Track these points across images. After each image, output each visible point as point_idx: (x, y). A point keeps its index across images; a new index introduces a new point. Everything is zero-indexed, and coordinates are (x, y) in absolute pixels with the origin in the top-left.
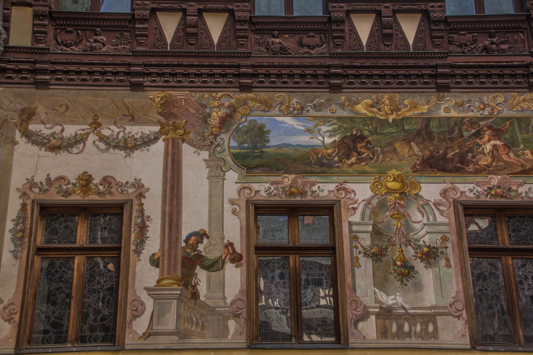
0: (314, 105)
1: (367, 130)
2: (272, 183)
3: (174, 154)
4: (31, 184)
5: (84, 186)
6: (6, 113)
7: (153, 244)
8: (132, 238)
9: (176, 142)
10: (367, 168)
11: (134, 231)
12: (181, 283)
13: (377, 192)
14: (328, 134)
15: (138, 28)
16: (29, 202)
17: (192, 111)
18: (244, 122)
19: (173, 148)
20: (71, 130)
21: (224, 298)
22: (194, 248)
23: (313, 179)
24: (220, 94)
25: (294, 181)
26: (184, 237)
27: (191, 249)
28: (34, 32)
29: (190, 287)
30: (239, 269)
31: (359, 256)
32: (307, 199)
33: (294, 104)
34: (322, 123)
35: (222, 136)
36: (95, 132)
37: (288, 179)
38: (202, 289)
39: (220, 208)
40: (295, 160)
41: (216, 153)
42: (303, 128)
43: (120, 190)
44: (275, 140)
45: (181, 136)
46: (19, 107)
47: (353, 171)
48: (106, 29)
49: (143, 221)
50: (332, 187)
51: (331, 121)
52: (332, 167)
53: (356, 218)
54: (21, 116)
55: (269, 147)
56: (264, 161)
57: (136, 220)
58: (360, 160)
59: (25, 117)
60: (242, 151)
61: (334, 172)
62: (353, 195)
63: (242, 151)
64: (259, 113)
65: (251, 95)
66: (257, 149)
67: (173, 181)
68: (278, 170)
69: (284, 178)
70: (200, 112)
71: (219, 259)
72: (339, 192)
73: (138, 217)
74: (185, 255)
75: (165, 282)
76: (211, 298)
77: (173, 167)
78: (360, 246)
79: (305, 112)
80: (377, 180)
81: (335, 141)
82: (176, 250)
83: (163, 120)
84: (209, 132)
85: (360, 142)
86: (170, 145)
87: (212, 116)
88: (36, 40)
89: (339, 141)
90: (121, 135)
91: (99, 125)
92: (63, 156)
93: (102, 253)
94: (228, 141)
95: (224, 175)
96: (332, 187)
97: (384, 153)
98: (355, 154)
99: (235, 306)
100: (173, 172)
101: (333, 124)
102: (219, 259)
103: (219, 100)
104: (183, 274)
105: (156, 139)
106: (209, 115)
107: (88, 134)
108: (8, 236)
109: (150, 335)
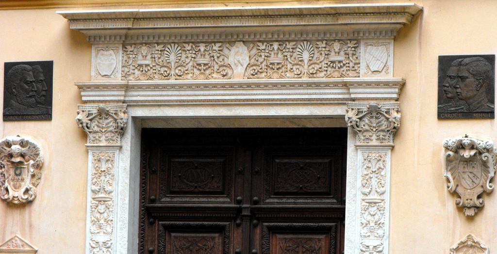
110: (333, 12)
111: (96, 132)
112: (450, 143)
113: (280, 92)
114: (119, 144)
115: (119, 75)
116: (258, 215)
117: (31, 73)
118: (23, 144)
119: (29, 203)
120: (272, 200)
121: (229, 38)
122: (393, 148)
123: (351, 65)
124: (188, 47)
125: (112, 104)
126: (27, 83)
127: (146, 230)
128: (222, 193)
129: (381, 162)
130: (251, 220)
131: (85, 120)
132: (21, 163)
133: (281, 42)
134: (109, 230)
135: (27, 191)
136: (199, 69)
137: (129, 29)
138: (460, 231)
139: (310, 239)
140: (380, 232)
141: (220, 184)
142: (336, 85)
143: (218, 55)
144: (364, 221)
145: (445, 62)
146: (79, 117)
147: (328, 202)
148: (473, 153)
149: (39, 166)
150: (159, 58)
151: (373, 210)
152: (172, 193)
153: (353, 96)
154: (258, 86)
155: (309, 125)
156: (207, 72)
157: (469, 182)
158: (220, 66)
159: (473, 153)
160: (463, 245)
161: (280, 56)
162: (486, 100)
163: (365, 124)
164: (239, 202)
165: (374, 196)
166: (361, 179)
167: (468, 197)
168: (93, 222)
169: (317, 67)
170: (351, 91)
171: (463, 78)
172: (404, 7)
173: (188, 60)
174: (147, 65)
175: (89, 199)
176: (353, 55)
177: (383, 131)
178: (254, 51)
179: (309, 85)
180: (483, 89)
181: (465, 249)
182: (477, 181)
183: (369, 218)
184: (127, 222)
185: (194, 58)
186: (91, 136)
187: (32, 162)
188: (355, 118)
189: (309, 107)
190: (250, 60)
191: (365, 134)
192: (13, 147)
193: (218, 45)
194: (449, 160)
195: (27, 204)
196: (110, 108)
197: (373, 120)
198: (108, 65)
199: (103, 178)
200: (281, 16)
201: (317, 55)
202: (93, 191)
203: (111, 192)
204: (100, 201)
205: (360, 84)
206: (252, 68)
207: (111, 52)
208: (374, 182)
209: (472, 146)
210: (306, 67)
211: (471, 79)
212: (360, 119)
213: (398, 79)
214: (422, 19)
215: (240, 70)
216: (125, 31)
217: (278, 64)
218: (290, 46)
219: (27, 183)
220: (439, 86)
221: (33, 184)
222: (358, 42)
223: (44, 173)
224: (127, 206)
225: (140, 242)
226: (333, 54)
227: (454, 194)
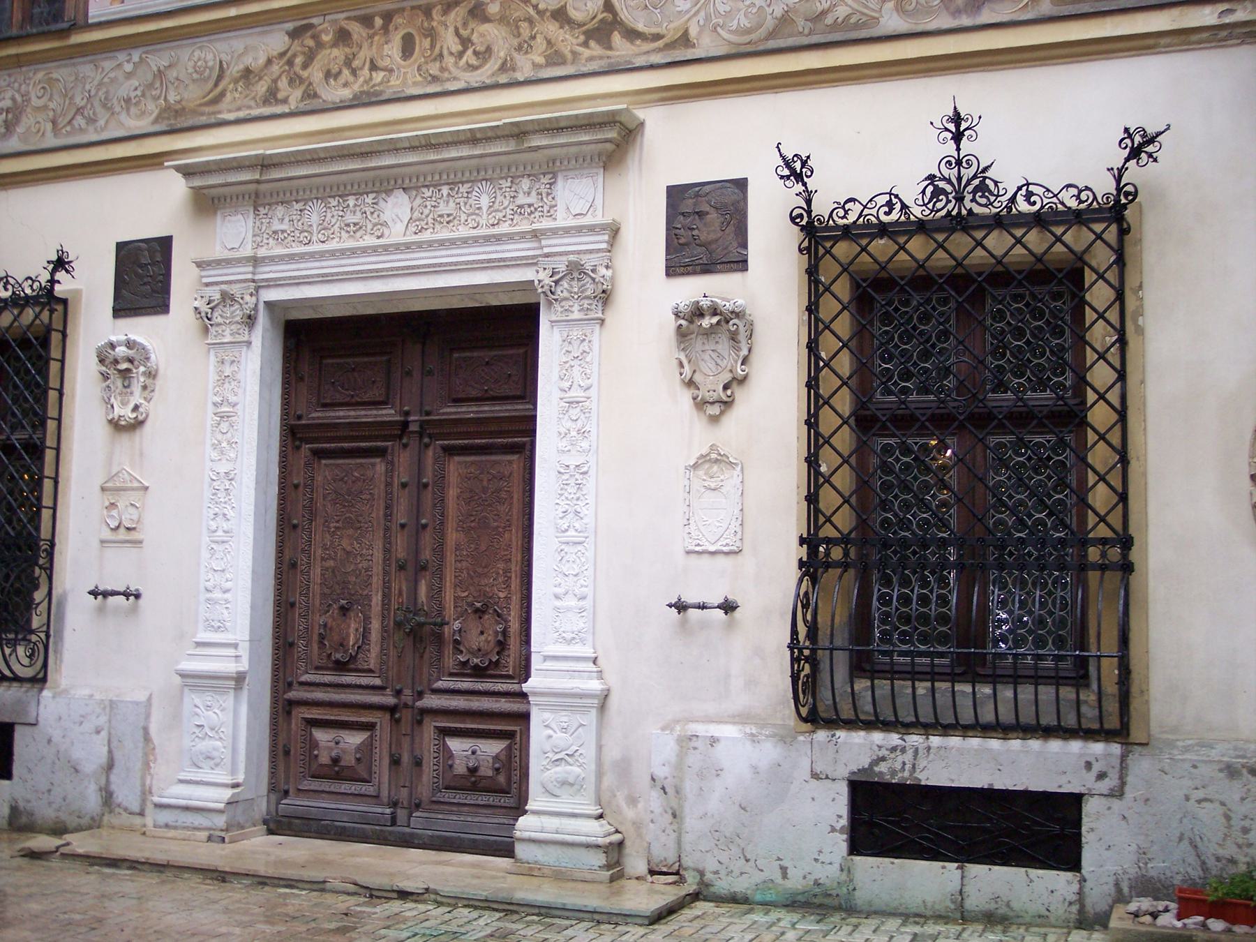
110: (516, 130)
111: (219, 325)
112: (681, 308)
113: (449, 252)
114: (246, 339)
115: (249, 247)
116: (430, 431)
117: (146, 253)
118: (130, 344)
119: (142, 423)
120: (448, 410)
121: (384, 185)
122: (602, 322)
123: (546, 208)
124: (334, 202)
125: (238, 286)
126: (141, 266)
127: (290, 458)
128: (386, 403)
129: (585, 343)
130: (421, 437)
131: (205, 308)
132: (128, 370)
133: (452, 184)
134: (233, 455)
135: (136, 408)
137: (258, 182)
138: (699, 436)
139: (496, 462)
140: (585, 444)
141: (383, 391)
142: (522, 236)
144: (563, 430)
145: (676, 194)
146: (197, 304)
147: (519, 408)
148: (715, 320)
149: (152, 375)
151: (574, 413)
152: (325, 405)
153: (546, 250)
154: (420, 245)
155: (495, 302)
156: (358, 234)
157: (712, 366)
158: (375, 225)
159: (715, 320)
160: (704, 460)
161: (452, 204)
162: (735, 244)
163: (561, 292)
164: (407, 414)
165: (576, 393)
166: (558, 369)
167: (710, 387)
168: (214, 447)
169: (500, 215)
170: (543, 243)
171: (701, 214)
172: (613, 113)
173: (334, 221)
174: (283, 231)
175: (210, 415)
176: (548, 194)
177: (588, 298)
178: (418, 201)
179: (488, 239)
180: (731, 229)
181: (707, 466)
182: (724, 363)
183: (569, 424)
184: (255, 444)
186: (213, 330)
187: (142, 369)
188: (548, 281)
189: (489, 272)
191: (563, 303)
192: (118, 349)
193: (372, 196)
194: (682, 334)
195: (137, 424)
196: (235, 290)
197: (575, 283)
198: (235, 233)
199: (226, 385)
200: (448, 144)
201: (500, 198)
202: (215, 404)
203: (235, 405)
204: (223, 417)
205: (554, 232)
207: (240, 216)
208: (576, 371)
209: (715, 311)
210: (485, 216)
211: (713, 215)
212: (556, 282)
213: (608, 219)
214: (642, 135)
216: (253, 187)
217: (449, 215)
218: (464, 189)
219: (137, 398)
220: (667, 229)
221: (145, 399)
222: (555, 176)
223: (159, 382)
224: (256, 423)
225: (281, 472)
226: (521, 195)
227: (691, 383)
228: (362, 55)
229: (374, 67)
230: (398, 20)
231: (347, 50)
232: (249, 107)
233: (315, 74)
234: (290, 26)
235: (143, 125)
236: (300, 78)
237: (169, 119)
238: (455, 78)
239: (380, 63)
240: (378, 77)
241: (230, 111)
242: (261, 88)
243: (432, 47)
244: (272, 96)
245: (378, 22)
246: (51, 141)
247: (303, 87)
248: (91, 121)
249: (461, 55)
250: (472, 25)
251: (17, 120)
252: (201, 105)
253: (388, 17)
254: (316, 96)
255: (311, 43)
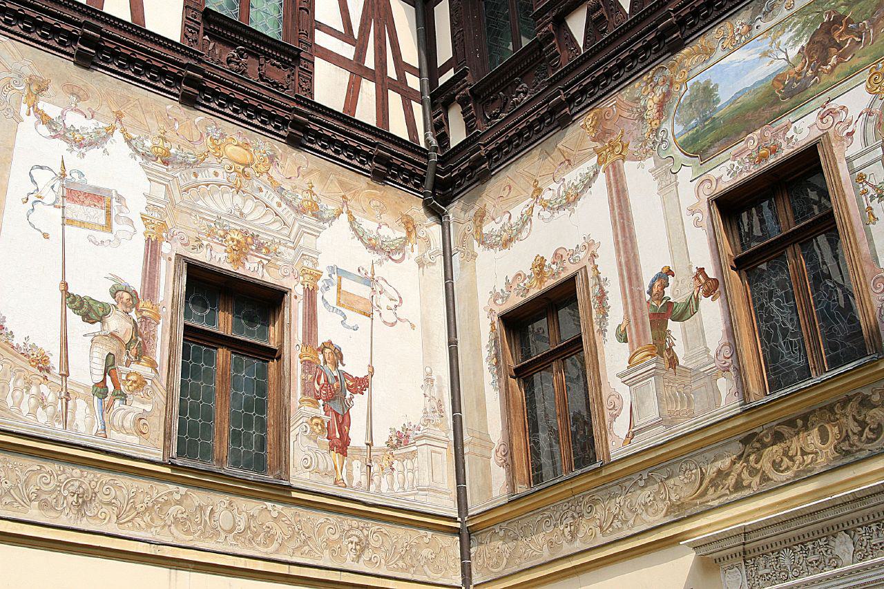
0: (764, 13)
1: (842, 5)
2: (735, 156)
3: (616, 182)
4: (496, 297)
5: (538, 274)
6: (464, 226)
7: (617, 314)
8: (594, 316)
9: (616, 165)
10: (856, 62)
11: (594, 306)
12: (655, 352)
13: (878, 90)
14: (791, 43)
15: (546, 51)
16: (496, 319)
17: (626, 114)
18: (684, 93)
19: (615, 175)
20: (517, 212)
21: (707, 350)
22: (661, 296)
23: (785, 120)
24: (651, 72)
25: (762, 136)
26: (647, 289)
27: (657, 299)
28: (466, 120)
29: (665, 353)
30: (718, 301)
31: (871, 205)
32: (783, 154)
33: (738, 29)
34: (780, 33)
35: (664, 126)
36: (538, 201)
37: (752, 142)
38: (679, 350)
39: (680, 226)
40: (756, 108)
41: (660, 154)
42: (758, 55)
43: (572, 261)
44: (725, 95)
45: (620, 154)
46: (472, 213)
47: (837, 77)
48: (524, 75)
49: (601, 289)
50: (813, 118)
51: (791, 22)
52: (807, 88)
53: (856, 146)
54: (475, 223)
55: (720, 108)
56: (719, 131)
57: (594, 290)
58: (841, 58)
59: (478, 222)
60: (690, 133)
61: (810, 94)
62: (844, 113)
63: (690, 133)
64: (700, 68)
65: (685, 51)
66: (707, 120)
67: (623, 218)
68: (738, 134)
69: (747, 142)
70: (635, 110)
71: (691, 298)
72: (824, 120)
73: (596, 285)
74: (652, 310)
75: (637, 358)
76: (691, 358)
77: (619, 201)
78: (870, 189)
79: (755, 32)
80: (874, 70)
81: (803, 47)
82: (641, 309)
83: (599, 145)
84: (649, 130)
85: (837, 29)
86: (611, 173)
87: (648, 106)
88: (469, 129)
89: (808, 44)
90: (562, 189)
91: (540, 190)
92: (515, 245)
93: (575, 348)
94: (674, 128)
95: (676, 178)
96: (813, 118)
97: (874, 25)
98: (834, 50)
99: (721, 357)
100: (620, 207)
101: (795, 24)
102: (691, 298)
103: (652, 81)
104: (654, 339)
105: (596, 173)
106: (645, 108)
107: (532, 207)
108: (486, 366)
109: (633, 435)
121: (830, 533)
136: (812, 567)
143: (826, 549)
150: (776, 565)
156: (820, 567)
185: (806, 557)
190: (855, 547)
206: (858, 554)
215: (848, 557)
228: (793, 446)
229: (804, 453)
230: (812, 419)
231: (783, 445)
232: (726, 495)
233: (765, 464)
234: (742, 436)
235: (659, 519)
236: (755, 469)
237: (674, 512)
238: (861, 450)
239: (808, 450)
240: (808, 459)
241: (713, 500)
242: (731, 481)
243: (840, 432)
244: (738, 486)
245: (800, 423)
246: (602, 540)
247: (759, 475)
248: (625, 522)
249: (861, 434)
250: (864, 412)
251: (577, 530)
252: (693, 499)
253: (805, 418)
254: (769, 479)
255: (758, 445)
